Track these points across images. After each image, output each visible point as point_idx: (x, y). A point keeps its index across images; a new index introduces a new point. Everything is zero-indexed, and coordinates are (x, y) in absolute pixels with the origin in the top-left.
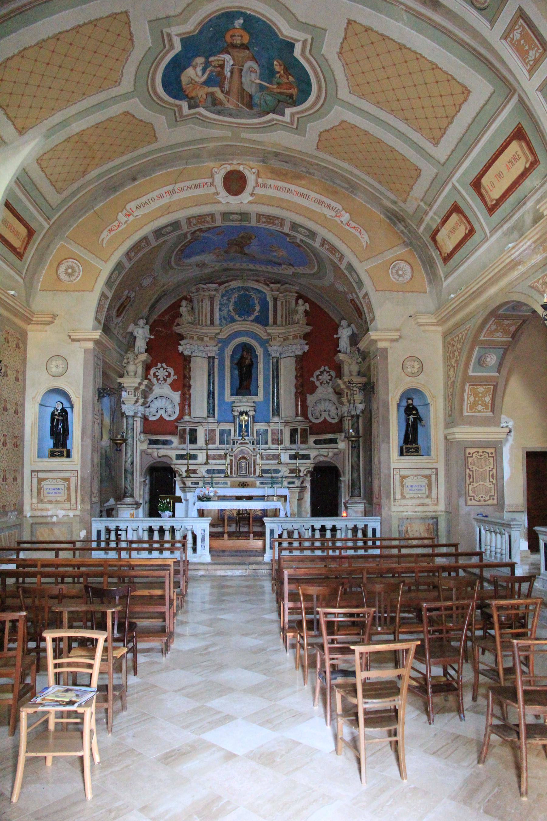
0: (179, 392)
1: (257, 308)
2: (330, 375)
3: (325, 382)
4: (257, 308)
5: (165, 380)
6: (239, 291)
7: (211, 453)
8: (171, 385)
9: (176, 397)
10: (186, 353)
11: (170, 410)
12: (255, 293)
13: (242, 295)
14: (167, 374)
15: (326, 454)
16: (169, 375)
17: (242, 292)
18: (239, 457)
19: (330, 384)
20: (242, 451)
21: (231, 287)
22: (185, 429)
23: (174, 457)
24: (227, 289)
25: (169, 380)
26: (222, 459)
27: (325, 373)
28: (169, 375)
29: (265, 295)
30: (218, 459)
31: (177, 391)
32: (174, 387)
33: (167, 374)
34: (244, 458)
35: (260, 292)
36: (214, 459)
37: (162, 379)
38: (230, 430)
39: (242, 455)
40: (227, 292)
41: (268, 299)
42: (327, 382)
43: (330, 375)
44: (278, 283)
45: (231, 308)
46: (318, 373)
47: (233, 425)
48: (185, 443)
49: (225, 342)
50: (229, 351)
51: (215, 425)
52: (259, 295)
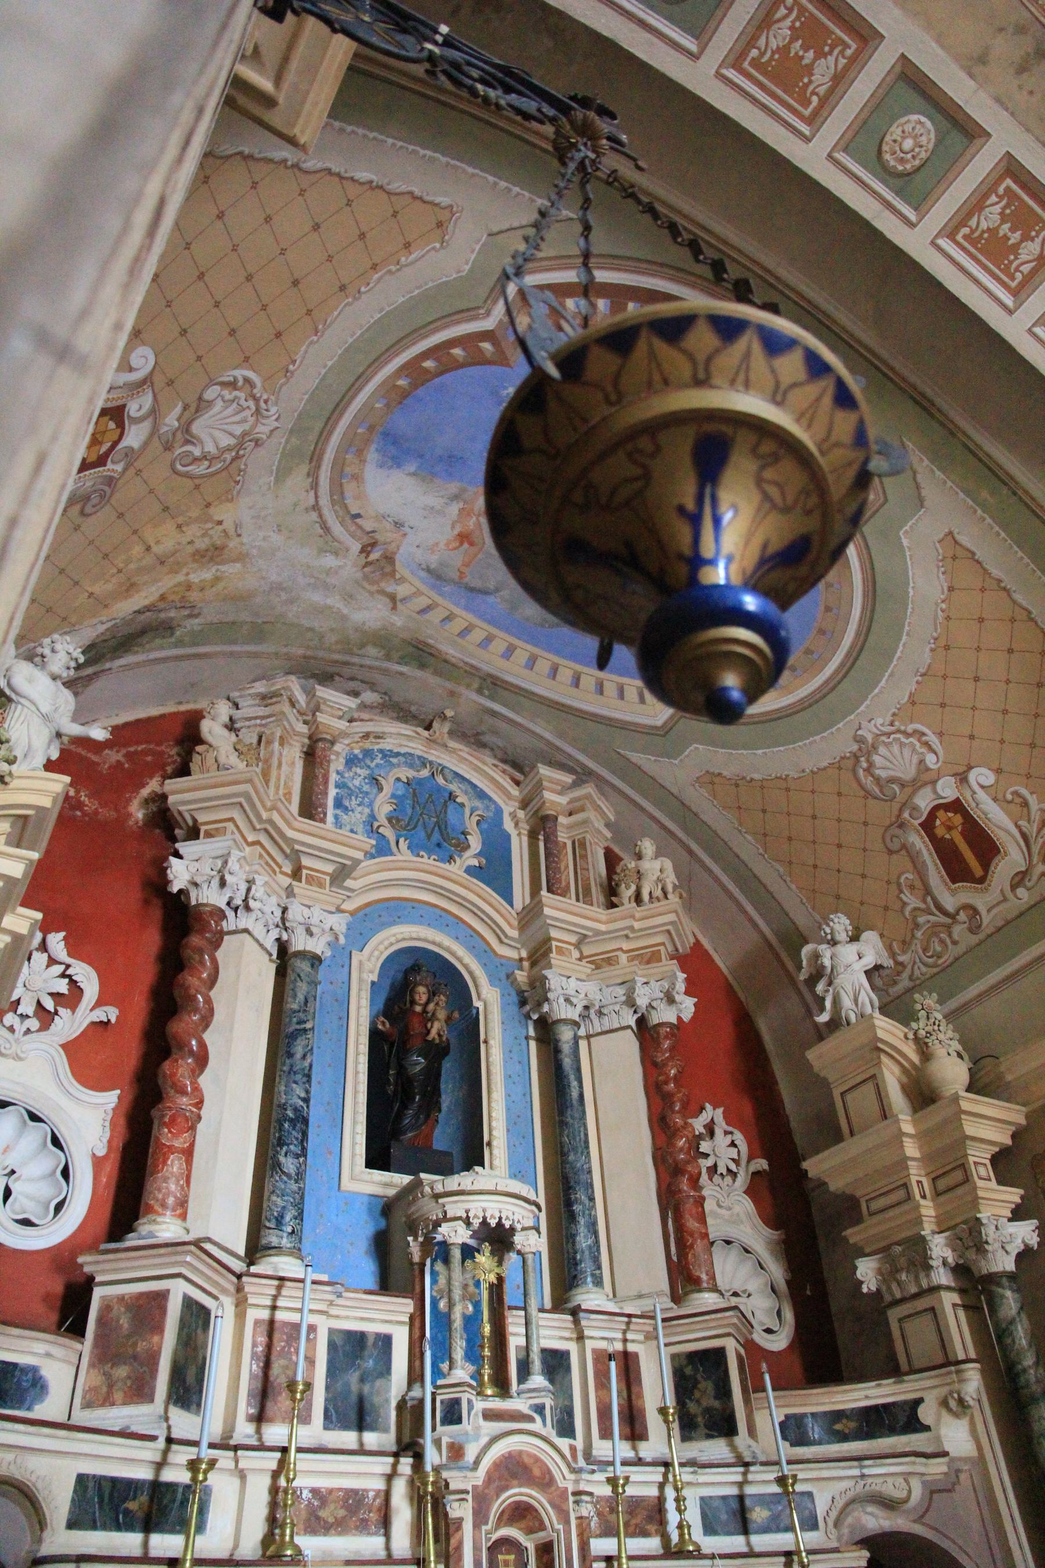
0: (111, 1098)
1: (475, 843)
2: (733, 1144)
3: (722, 1169)
4: (475, 843)
5: (45, 1017)
6: (411, 766)
7: (311, 1475)
8: (74, 1050)
9: (91, 1120)
10: (210, 896)
11: (33, 1189)
12: (466, 793)
13: (420, 782)
14: (63, 987)
15: (894, 1489)
16: (72, 997)
17: (425, 773)
18: (495, 1509)
19: (740, 1179)
20: (514, 1469)
21: (387, 744)
22: (162, 1297)
23: (59, 1501)
24: (367, 745)
25: (70, 1024)
26: (363, 1527)
27: (719, 1132)
28: (72, 997)
29: (499, 811)
30: (339, 1527)
31: (98, 1085)
32: (84, 1059)
33: (63, 987)
34: (521, 1513)
35: (482, 795)
36: (316, 1525)
37: (27, 1007)
38: (386, 1341)
39: (518, 1493)
40: (368, 753)
41: (508, 825)
42: (729, 1170)
43: (733, 1144)
44: (570, 770)
45: (383, 808)
46: (698, 1124)
47: (406, 1306)
48: (140, 1391)
49: (367, 920)
50: (368, 966)
51: (315, 1299)
52: (477, 803)
